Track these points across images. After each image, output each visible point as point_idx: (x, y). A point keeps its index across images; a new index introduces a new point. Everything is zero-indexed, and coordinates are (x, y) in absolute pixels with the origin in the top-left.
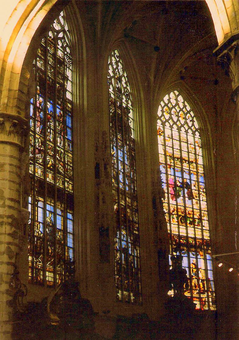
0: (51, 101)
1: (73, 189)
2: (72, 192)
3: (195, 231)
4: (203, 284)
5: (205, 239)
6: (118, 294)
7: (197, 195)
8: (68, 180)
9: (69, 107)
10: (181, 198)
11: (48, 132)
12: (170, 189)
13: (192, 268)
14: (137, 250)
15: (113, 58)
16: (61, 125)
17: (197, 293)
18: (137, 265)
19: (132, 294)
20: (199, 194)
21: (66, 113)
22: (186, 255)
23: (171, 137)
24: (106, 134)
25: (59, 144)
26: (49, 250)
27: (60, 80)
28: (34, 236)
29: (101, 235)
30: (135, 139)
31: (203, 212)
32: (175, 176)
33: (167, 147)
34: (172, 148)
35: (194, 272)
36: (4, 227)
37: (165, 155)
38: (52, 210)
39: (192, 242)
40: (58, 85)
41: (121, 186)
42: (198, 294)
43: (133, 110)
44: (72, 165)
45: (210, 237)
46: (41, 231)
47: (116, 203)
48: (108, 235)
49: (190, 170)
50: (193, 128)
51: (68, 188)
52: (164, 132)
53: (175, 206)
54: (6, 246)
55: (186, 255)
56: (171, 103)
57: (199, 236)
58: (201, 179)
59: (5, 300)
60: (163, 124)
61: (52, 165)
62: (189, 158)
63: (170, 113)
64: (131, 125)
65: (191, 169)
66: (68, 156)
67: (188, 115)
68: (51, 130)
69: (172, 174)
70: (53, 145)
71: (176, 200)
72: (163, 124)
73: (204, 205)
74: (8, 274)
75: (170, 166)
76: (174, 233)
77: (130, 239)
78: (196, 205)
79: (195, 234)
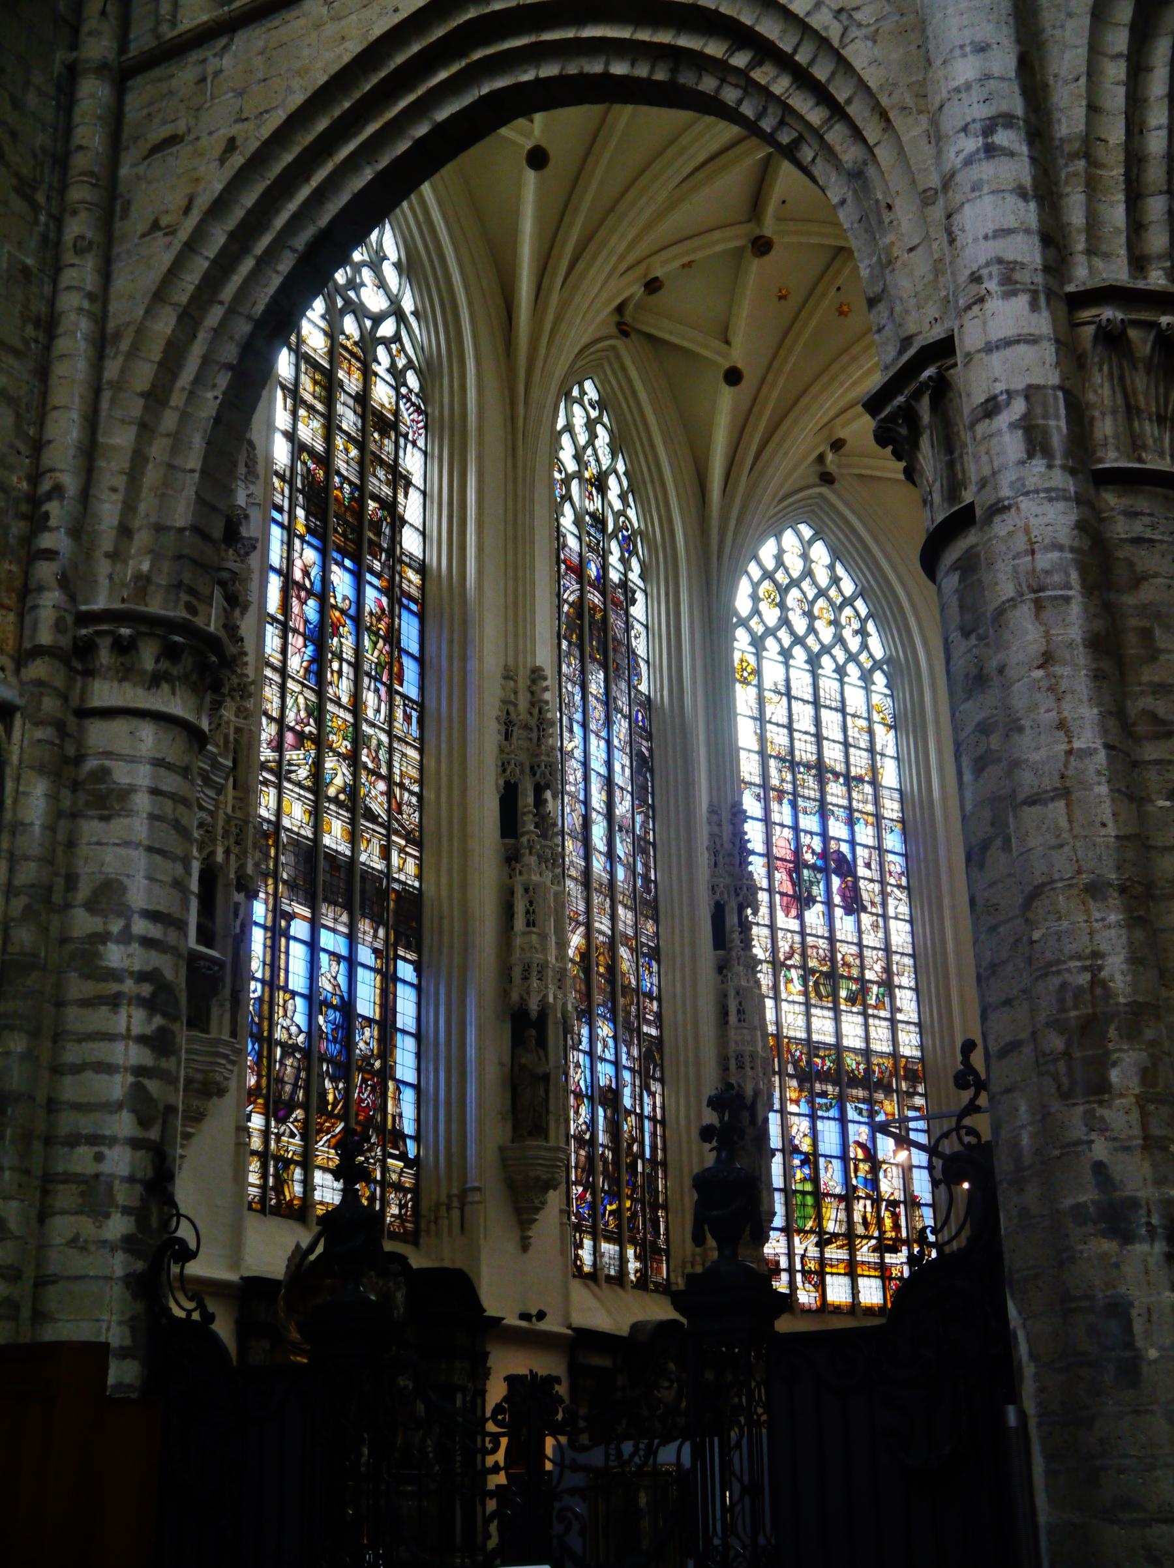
0: (347, 563)
1: (419, 877)
2: (417, 884)
3: (866, 1026)
4: (895, 1217)
5: (903, 1056)
6: (580, 1252)
7: (878, 899)
8: (403, 842)
9: (410, 581)
10: (819, 908)
11: (332, 672)
12: (777, 876)
13: (855, 1159)
14: (652, 1095)
15: (576, 408)
16: (381, 644)
17: (875, 1249)
18: (654, 1148)
19: (630, 1252)
20: (884, 894)
21: (401, 605)
22: (833, 1113)
23: (783, 690)
24: (545, 679)
25: (370, 714)
26: (324, 1093)
27: (379, 483)
28: (271, 1042)
29: (518, 1041)
30: (652, 695)
31: (896, 958)
32: (796, 828)
33: (769, 726)
34: (785, 731)
35: (861, 1174)
36: (123, 1011)
37: (763, 754)
38: (343, 951)
39: (854, 1066)
40: (372, 505)
41: (598, 864)
42: (873, 1251)
43: (646, 595)
44: (416, 788)
45: (922, 1047)
46: (298, 1026)
47: (578, 924)
48: (542, 1042)
49: (850, 809)
50: (863, 657)
51: (400, 870)
52: (758, 672)
53: (797, 938)
54: (130, 1079)
55: (833, 1113)
56: (786, 570)
57: (881, 1045)
58: (893, 841)
59: (119, 1272)
60: (758, 643)
61: (342, 790)
62: (847, 763)
63: (782, 606)
64: (640, 647)
65: (855, 804)
66: (404, 755)
67: (848, 611)
68: (345, 666)
69: (788, 821)
70: (349, 717)
71: (800, 917)
72: (758, 643)
73: (901, 935)
74: (131, 1179)
75: (781, 793)
76: (792, 1034)
77: (628, 1053)
79: (867, 1039)
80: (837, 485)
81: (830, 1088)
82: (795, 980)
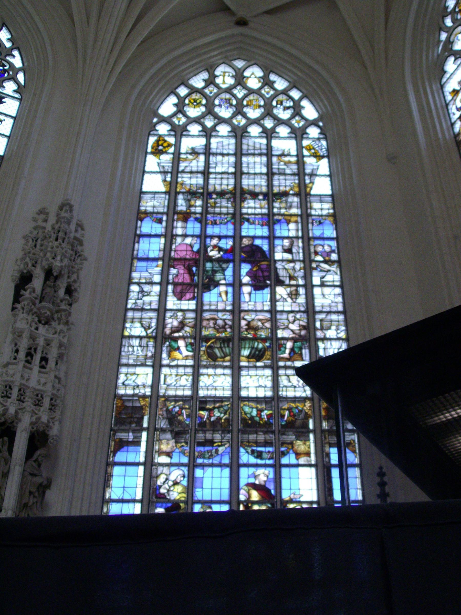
39: (254, 413)
78: (289, 300)
80: (251, 24)
81: (218, 437)
82: (183, 349)
